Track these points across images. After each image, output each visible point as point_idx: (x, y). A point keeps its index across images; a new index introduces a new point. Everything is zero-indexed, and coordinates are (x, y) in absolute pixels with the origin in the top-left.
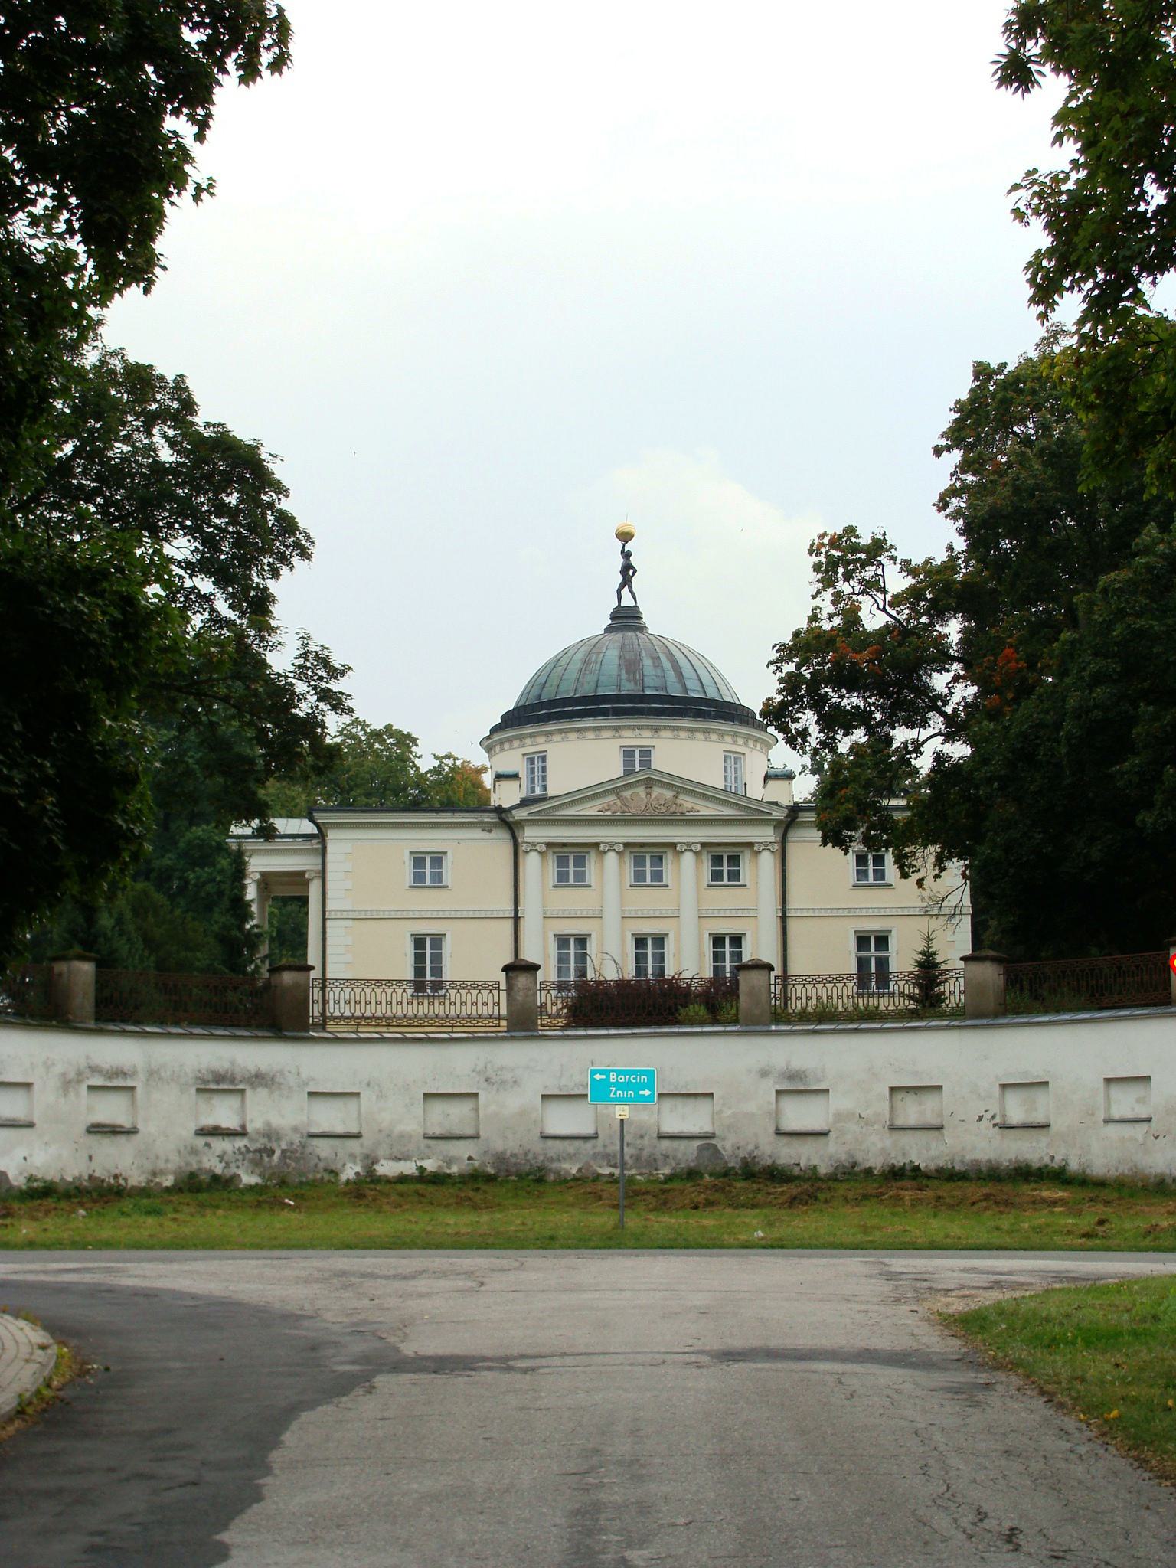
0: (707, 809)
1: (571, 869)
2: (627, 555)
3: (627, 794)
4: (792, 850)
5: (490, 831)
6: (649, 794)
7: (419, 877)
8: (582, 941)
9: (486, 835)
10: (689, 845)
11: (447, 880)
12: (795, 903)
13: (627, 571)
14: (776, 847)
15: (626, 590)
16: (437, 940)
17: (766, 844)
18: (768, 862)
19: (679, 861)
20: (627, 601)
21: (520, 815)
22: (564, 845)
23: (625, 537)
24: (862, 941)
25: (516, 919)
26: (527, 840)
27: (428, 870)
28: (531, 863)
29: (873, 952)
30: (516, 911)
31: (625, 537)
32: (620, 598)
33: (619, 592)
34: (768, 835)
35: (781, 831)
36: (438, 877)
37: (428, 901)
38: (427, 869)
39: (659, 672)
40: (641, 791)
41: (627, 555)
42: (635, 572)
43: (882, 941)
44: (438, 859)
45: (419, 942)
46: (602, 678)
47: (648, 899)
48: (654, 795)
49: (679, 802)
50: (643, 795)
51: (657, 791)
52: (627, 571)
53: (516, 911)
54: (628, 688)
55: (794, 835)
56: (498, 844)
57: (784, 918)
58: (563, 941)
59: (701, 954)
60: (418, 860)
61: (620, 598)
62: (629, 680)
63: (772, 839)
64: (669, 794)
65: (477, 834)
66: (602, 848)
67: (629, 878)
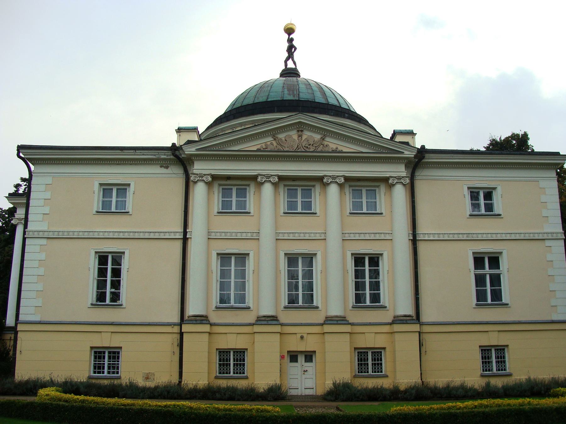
0: (347, 148)
1: (234, 199)
2: (290, 41)
3: (282, 136)
4: (421, 187)
5: (167, 167)
6: (300, 136)
7: (106, 205)
8: (242, 258)
9: (164, 170)
10: (334, 177)
11: (129, 207)
12: (423, 229)
13: (291, 49)
14: (408, 181)
15: (290, 61)
16: (118, 258)
17: (399, 178)
18: (400, 193)
19: (325, 193)
20: (290, 65)
21: (190, 150)
22: (229, 178)
23: (289, 31)
24: (478, 261)
25: (185, 240)
26: (195, 171)
27: (114, 200)
28: (199, 191)
29: (487, 270)
30: (185, 233)
31: (289, 31)
32: (286, 65)
33: (286, 62)
34: (401, 170)
35: (410, 170)
36: (121, 204)
37: (113, 225)
38: (113, 197)
39: (310, 91)
40: (294, 134)
41: (290, 41)
42: (296, 49)
43: (495, 261)
44: (123, 189)
45: (102, 259)
46: (271, 94)
47: (299, 224)
48: (304, 137)
49: (326, 143)
50: (295, 137)
51: (307, 134)
52: (291, 49)
53: (185, 233)
54: (288, 97)
55: (421, 174)
56: (173, 178)
57: (414, 241)
58: (224, 258)
59: (345, 271)
60: (106, 189)
61: (286, 65)
62: (289, 94)
63: (404, 174)
64: (317, 137)
65: (156, 170)
66: (259, 179)
67: (283, 207)
